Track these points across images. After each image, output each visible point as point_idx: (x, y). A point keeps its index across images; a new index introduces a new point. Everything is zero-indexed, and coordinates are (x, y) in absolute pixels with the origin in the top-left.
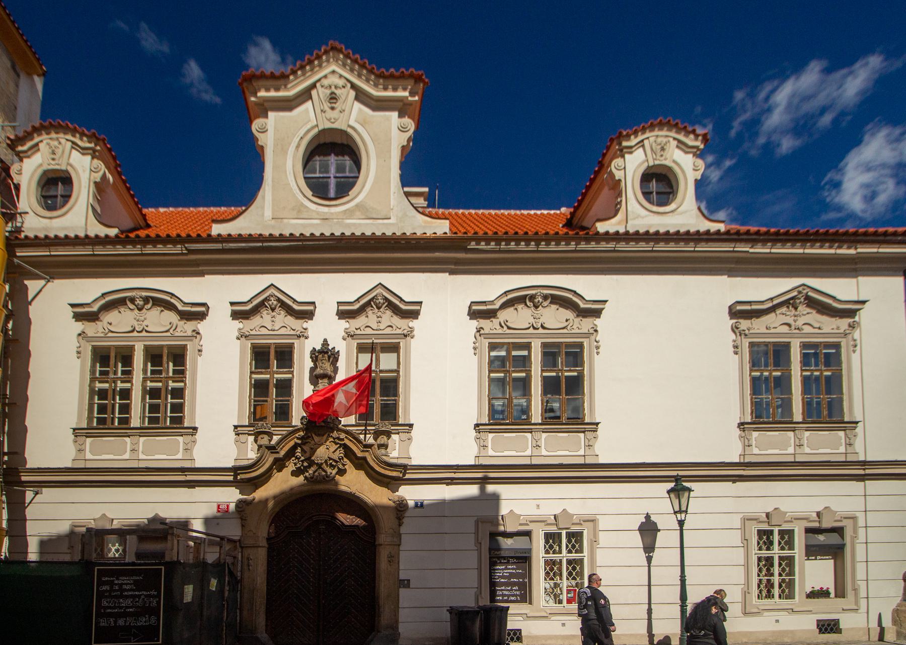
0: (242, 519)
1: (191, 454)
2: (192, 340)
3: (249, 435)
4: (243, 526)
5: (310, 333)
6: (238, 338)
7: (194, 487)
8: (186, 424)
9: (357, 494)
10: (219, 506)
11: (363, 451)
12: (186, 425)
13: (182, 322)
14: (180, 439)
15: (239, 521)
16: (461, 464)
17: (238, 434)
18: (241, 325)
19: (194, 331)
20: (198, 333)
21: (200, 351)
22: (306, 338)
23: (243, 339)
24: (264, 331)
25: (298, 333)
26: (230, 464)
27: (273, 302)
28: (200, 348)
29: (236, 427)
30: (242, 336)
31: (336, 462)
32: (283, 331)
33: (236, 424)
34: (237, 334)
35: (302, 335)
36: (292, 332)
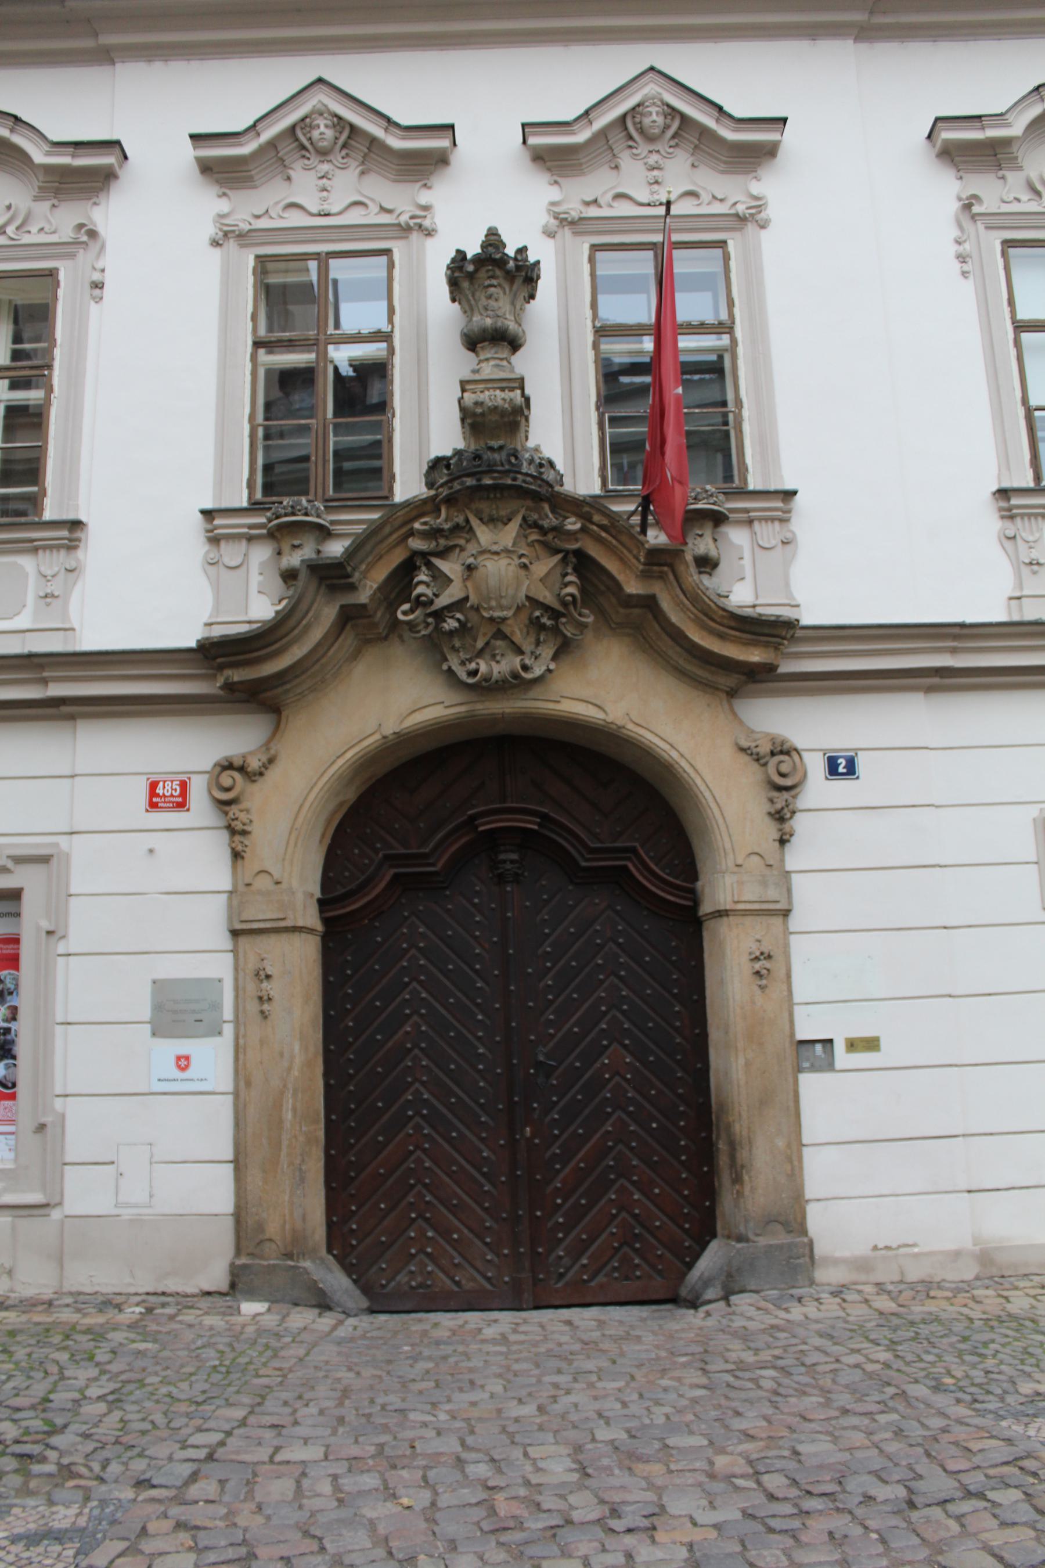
0: (232, 831)
1: (65, 614)
2: (72, 256)
3: (250, 539)
4: (237, 856)
5: (439, 219)
6: (215, 243)
7: (72, 717)
8: (49, 514)
9: (633, 730)
10: (153, 786)
11: (646, 575)
12: (48, 515)
13: (45, 206)
14: (27, 563)
15: (225, 835)
16: (970, 619)
17: (215, 540)
18: (223, 206)
19: (81, 226)
20: (93, 234)
21: (98, 286)
22: (429, 233)
23: (232, 244)
24: (296, 219)
25: (404, 219)
26: (187, 636)
27: (323, 132)
28: (96, 277)
29: (208, 514)
30: (226, 236)
31: (555, 614)
32: (355, 217)
33: (209, 505)
34: (210, 230)
35: (418, 227)
36: (385, 219)
